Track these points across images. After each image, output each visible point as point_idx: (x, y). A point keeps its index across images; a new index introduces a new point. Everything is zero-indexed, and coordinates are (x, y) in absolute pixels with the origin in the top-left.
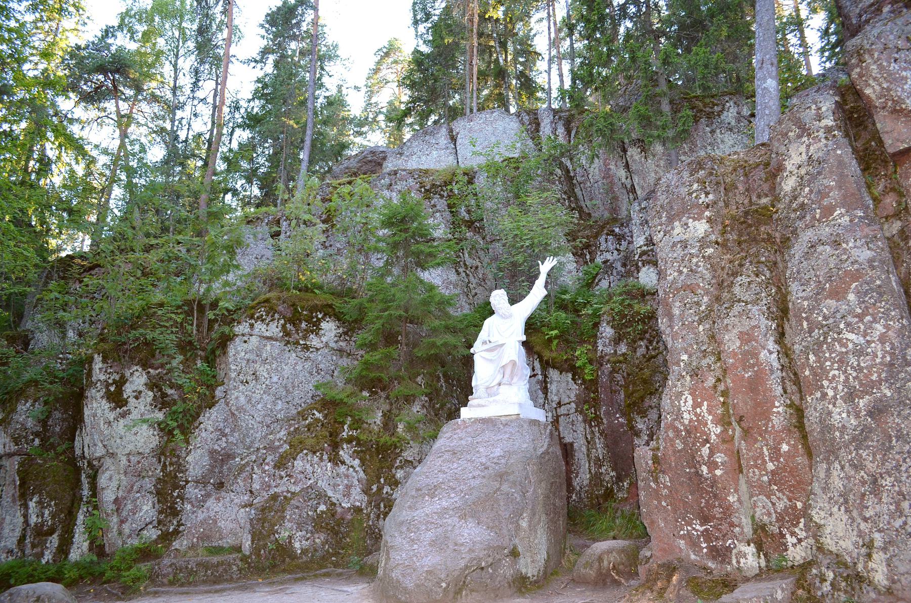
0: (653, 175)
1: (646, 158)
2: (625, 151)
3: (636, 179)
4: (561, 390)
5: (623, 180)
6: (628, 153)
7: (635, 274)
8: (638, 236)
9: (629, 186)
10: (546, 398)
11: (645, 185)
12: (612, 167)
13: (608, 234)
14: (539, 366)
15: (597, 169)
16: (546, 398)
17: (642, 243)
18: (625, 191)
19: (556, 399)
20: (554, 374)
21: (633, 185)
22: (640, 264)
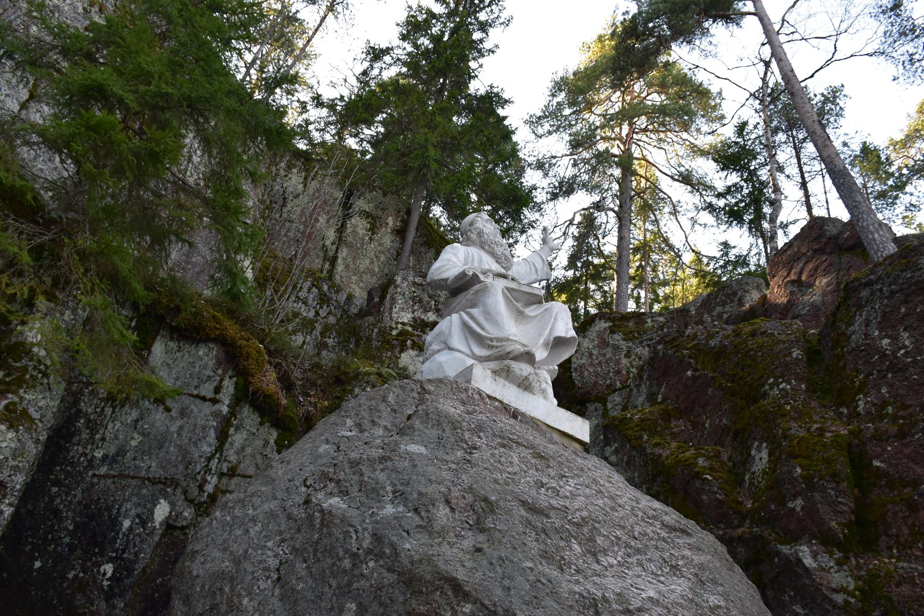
0: (367, 262)
1: (371, 239)
2: (347, 216)
3: (344, 253)
4: (249, 450)
5: (328, 243)
6: (353, 220)
7: (397, 350)
8: (402, 309)
9: (331, 254)
10: (220, 449)
11: (352, 266)
12: (321, 220)
13: (313, 285)
14: (231, 390)
15: (300, 209)
16: (220, 449)
17: (406, 321)
18: (321, 254)
19: (233, 458)
20: (248, 416)
21: (335, 258)
22: (409, 342)
